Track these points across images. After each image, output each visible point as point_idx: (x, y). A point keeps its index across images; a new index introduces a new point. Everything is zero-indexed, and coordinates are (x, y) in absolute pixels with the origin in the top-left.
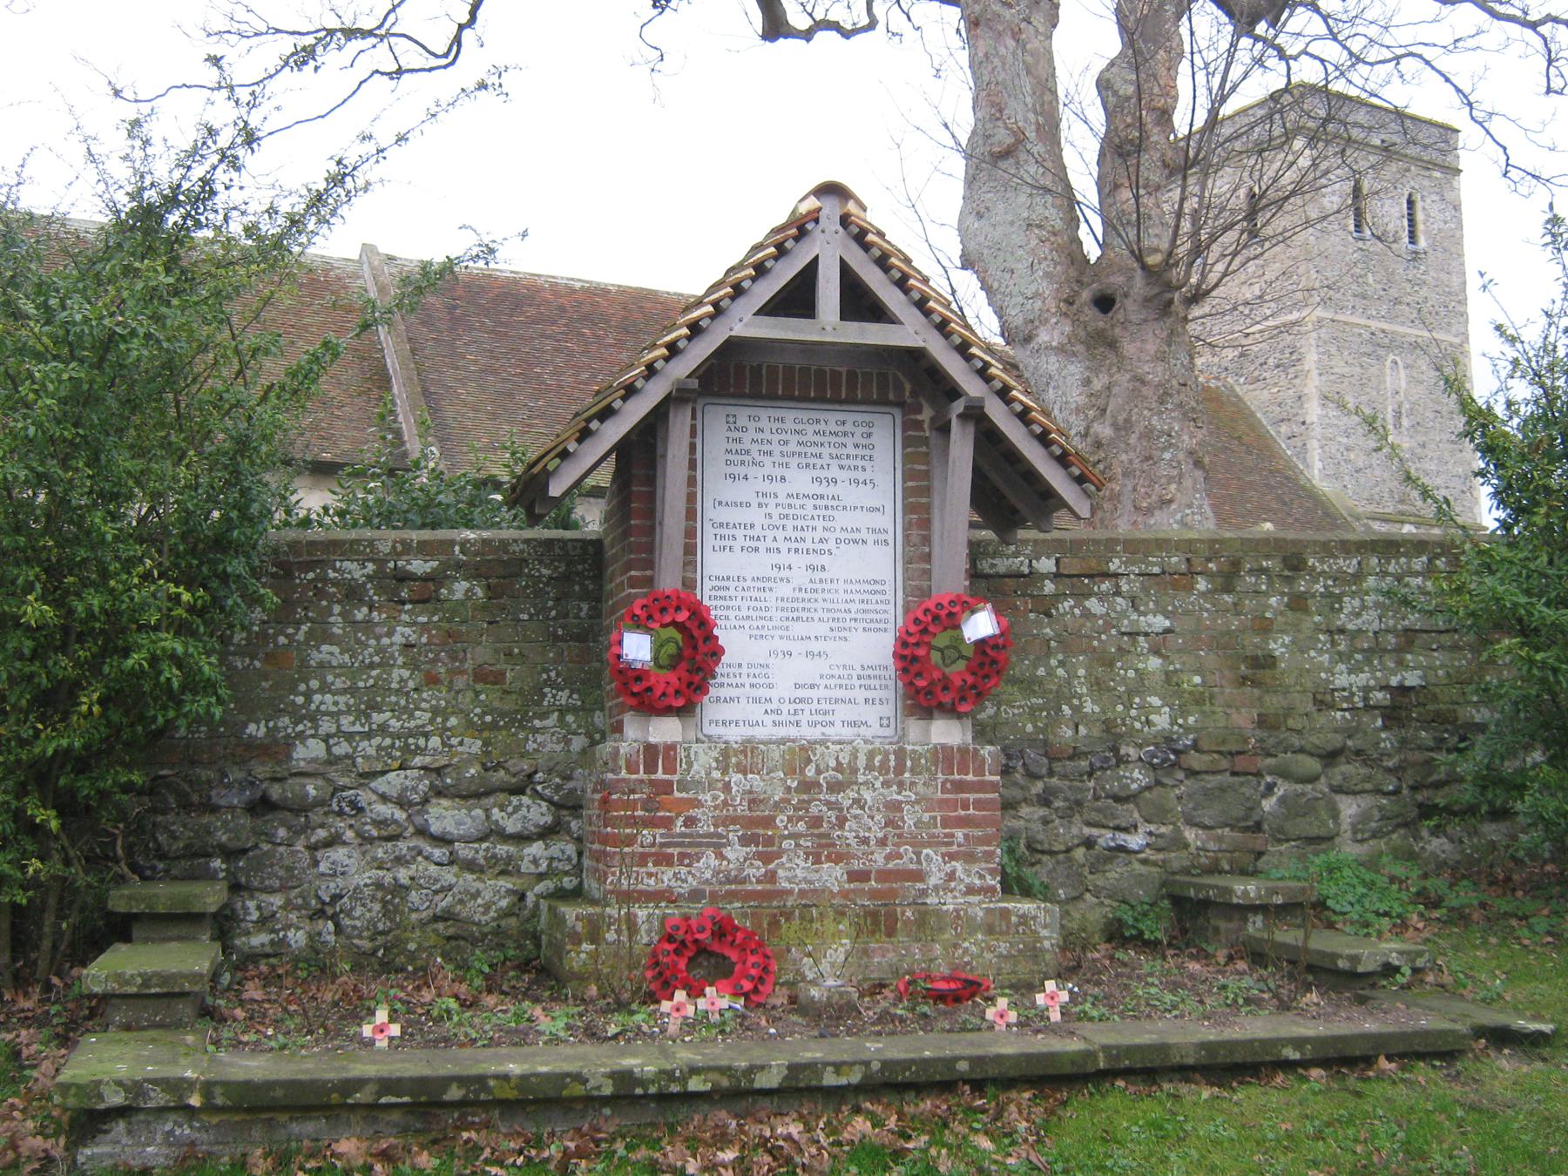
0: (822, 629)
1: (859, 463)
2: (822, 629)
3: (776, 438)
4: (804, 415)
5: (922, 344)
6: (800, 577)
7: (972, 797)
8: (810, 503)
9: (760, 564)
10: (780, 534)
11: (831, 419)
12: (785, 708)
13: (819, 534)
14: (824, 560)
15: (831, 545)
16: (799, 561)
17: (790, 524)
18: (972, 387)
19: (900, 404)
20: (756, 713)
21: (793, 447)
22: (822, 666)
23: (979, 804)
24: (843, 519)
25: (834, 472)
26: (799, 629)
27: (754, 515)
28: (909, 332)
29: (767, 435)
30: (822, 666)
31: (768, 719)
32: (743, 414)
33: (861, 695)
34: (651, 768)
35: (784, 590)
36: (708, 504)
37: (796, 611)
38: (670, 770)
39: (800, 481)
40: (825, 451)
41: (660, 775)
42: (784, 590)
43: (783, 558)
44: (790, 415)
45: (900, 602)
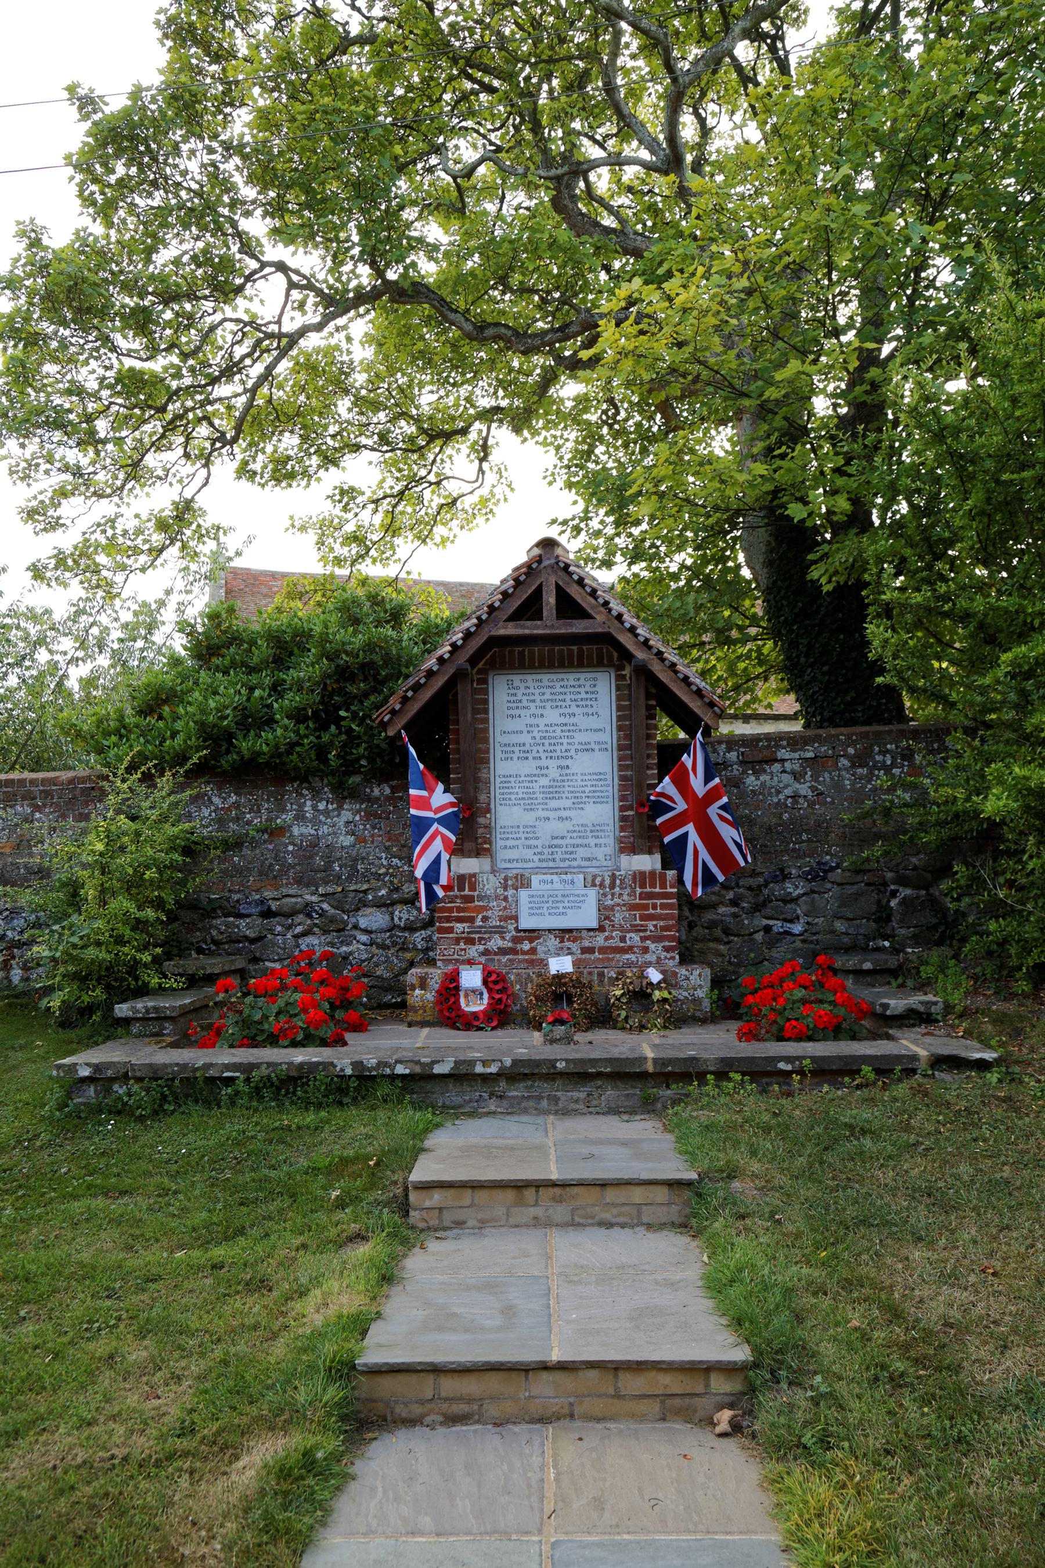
0: (568, 803)
1: (589, 703)
2: (568, 803)
3: (537, 691)
4: (554, 677)
5: (606, 630)
6: (554, 773)
7: (659, 902)
8: (559, 729)
9: (529, 767)
10: (541, 748)
11: (570, 678)
12: (546, 851)
13: (565, 747)
14: (569, 762)
15: (573, 753)
16: (553, 764)
17: (547, 742)
18: (640, 655)
19: (611, 664)
20: (528, 854)
21: (547, 696)
22: (568, 825)
23: (663, 906)
24: (579, 737)
25: (574, 709)
26: (553, 804)
27: (526, 738)
28: (598, 624)
29: (532, 690)
30: (568, 825)
31: (536, 858)
32: (517, 679)
33: (592, 841)
34: (461, 888)
35: (544, 781)
36: (497, 734)
37: (553, 792)
38: (473, 888)
39: (553, 716)
40: (568, 697)
41: (467, 892)
42: (544, 781)
43: (543, 763)
44: (545, 678)
45: (616, 787)
